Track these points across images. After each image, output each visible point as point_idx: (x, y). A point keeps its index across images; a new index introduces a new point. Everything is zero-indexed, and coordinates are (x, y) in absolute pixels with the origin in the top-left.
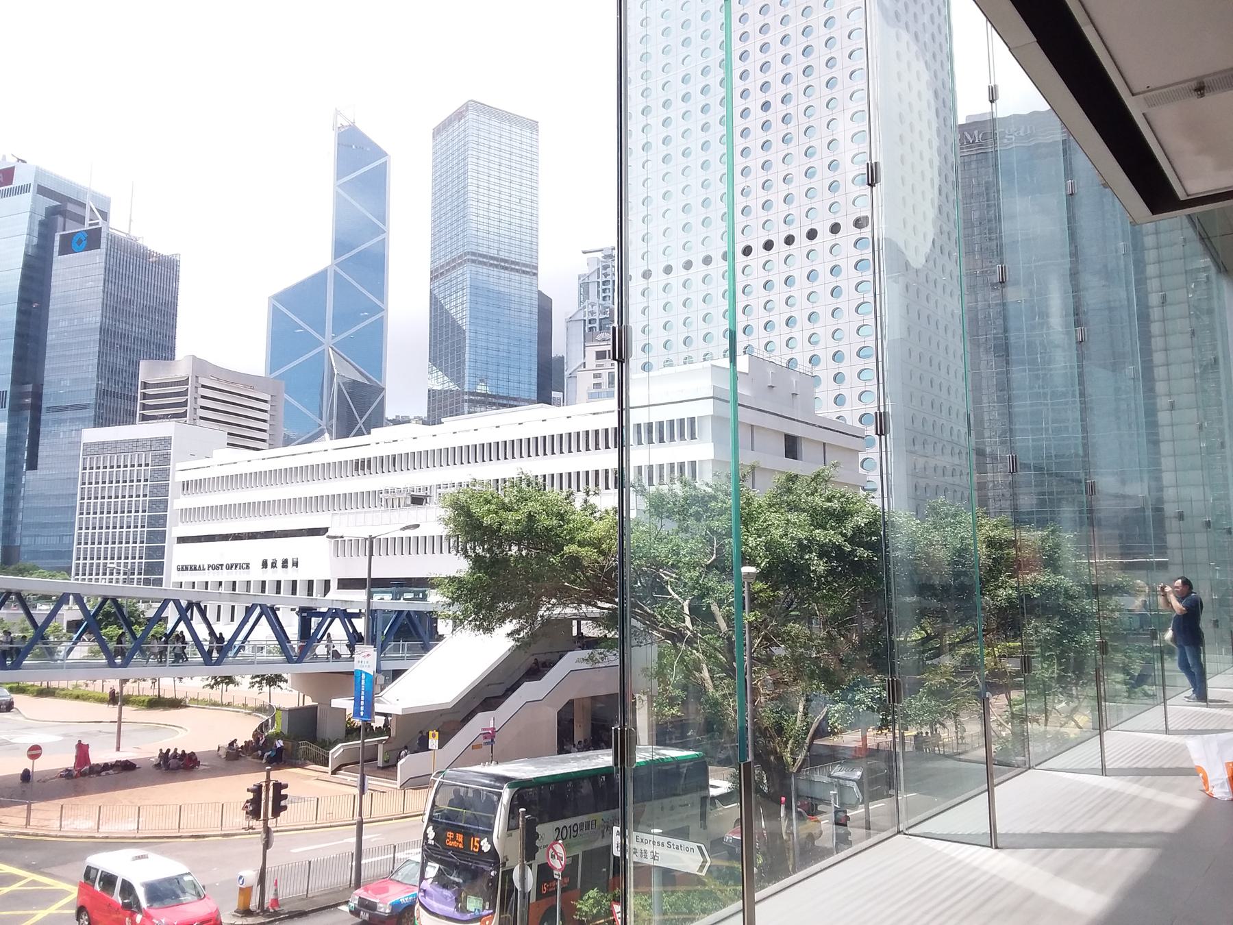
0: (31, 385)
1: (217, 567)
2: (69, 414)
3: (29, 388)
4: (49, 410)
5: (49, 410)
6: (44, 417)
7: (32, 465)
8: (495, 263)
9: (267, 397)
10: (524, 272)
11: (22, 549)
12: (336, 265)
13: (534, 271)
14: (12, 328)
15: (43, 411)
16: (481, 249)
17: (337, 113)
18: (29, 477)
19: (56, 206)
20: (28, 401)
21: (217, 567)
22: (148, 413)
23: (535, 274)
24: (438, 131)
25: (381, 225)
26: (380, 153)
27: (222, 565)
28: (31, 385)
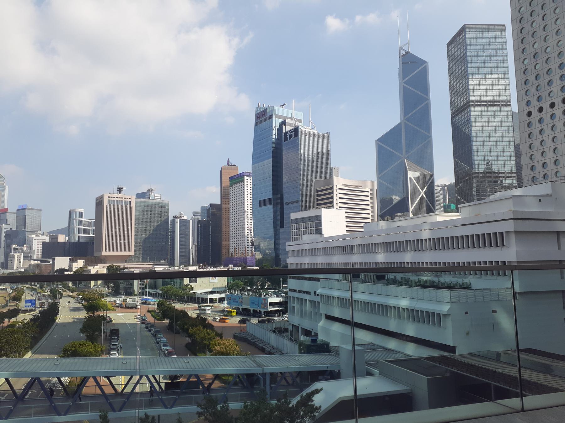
0: (279, 195)
1: (300, 292)
2: (292, 205)
3: (279, 196)
4: (288, 203)
5: (288, 203)
6: (285, 207)
7: (282, 226)
8: (485, 104)
9: (369, 190)
10: (503, 105)
11: (281, 259)
12: (405, 120)
13: (509, 104)
14: (271, 173)
15: (284, 204)
16: (476, 98)
17: (401, 49)
18: (281, 230)
19: (283, 121)
20: (279, 201)
21: (300, 292)
22: (319, 202)
23: (510, 105)
24: (449, 45)
25: (425, 96)
26: (423, 62)
27: (302, 291)
28: (279, 195)
